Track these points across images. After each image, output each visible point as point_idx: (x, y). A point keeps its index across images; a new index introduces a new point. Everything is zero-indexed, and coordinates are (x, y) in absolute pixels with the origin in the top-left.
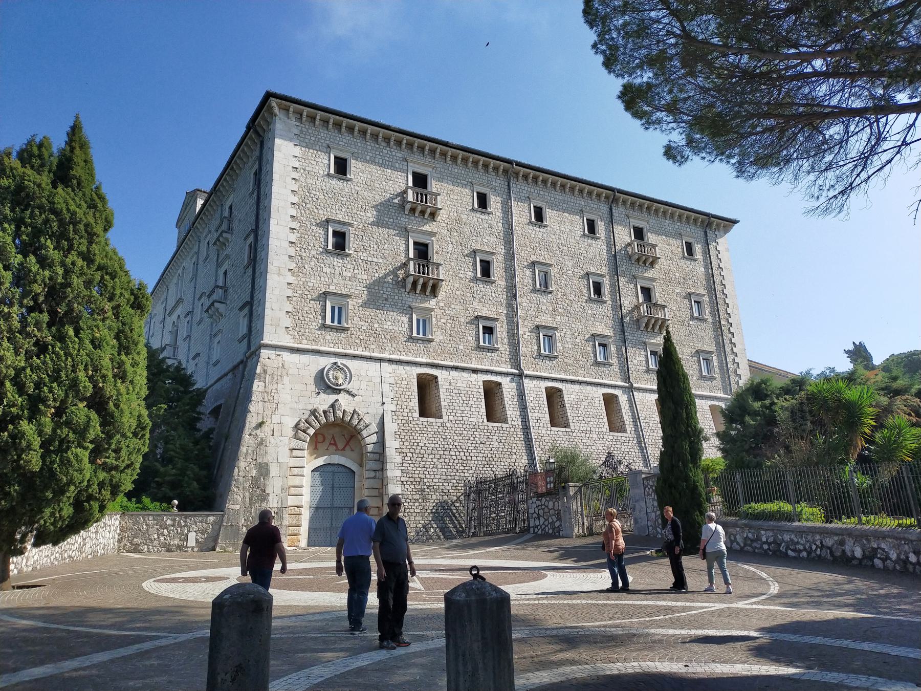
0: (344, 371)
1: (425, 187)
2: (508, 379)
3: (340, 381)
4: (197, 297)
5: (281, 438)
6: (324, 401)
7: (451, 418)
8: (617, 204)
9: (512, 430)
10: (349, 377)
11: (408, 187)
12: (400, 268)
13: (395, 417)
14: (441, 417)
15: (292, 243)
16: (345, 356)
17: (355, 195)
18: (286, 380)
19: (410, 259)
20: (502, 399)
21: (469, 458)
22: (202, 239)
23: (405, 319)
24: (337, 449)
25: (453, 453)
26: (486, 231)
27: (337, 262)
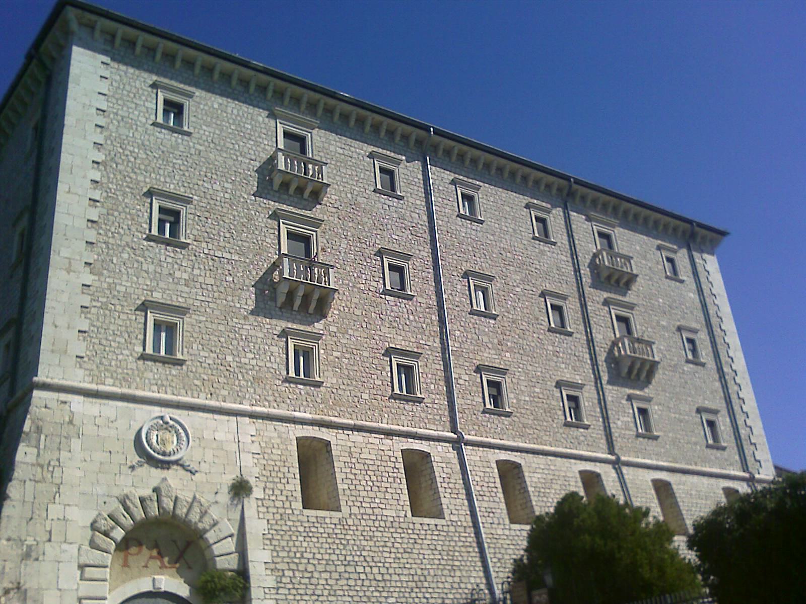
0: (177, 432)
3: (169, 448)
7: (355, 510)
9: (452, 529)
13: (262, 509)
14: (338, 509)
15: (93, 222)
18: (76, 444)
19: (281, 256)
20: (433, 480)
21: (387, 577)
25: (360, 569)
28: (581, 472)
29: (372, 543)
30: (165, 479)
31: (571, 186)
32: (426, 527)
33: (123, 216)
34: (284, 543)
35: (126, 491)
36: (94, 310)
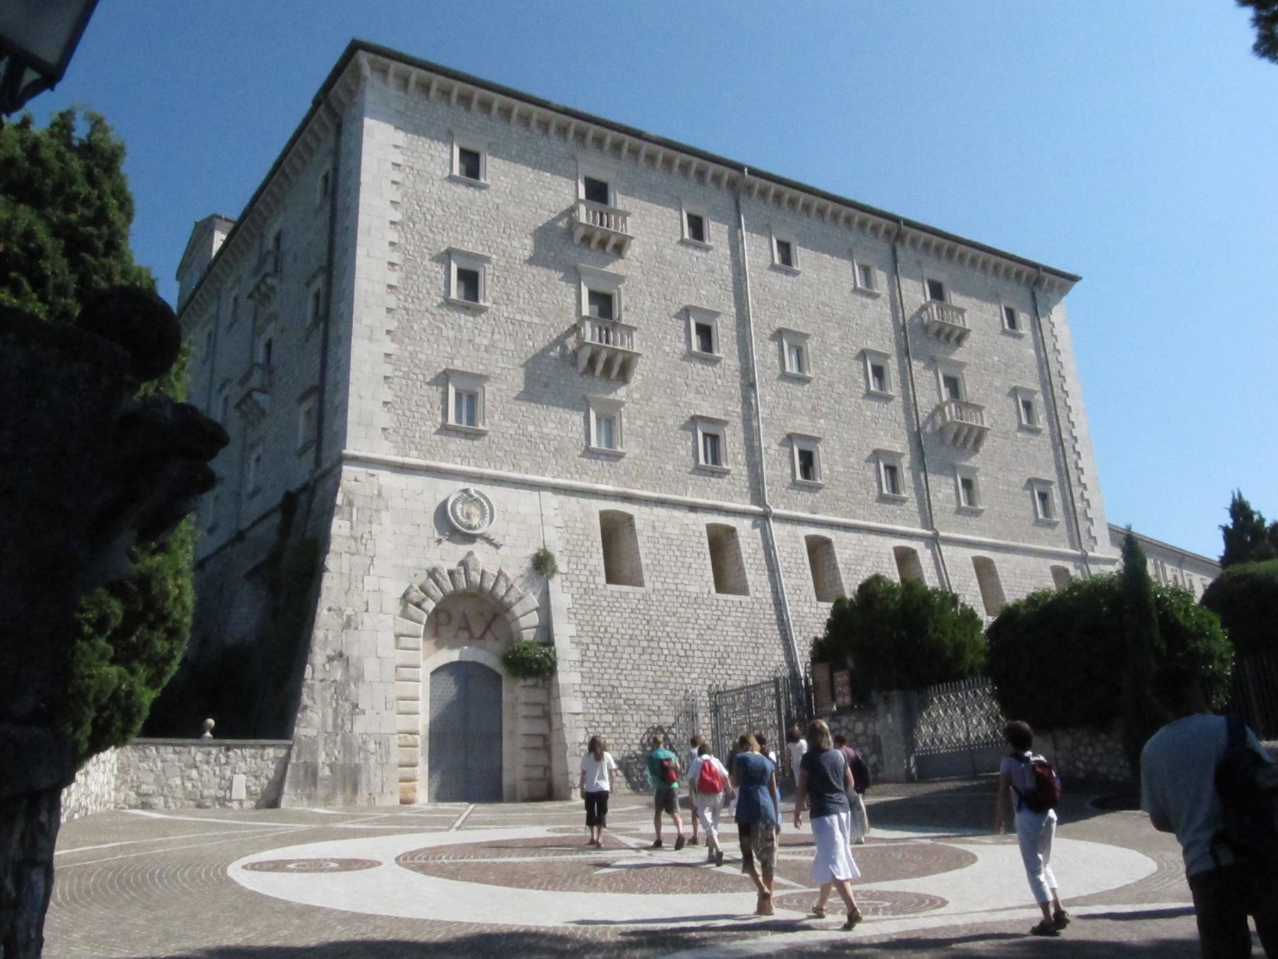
0: (481, 504)
2: (748, 522)
5: (381, 616)
6: (449, 556)
7: (658, 585)
8: (903, 242)
10: (488, 512)
11: (578, 201)
12: (568, 334)
14: (641, 584)
15: (390, 287)
16: (480, 478)
17: (493, 212)
18: (386, 517)
19: (583, 319)
21: (690, 653)
23: (578, 418)
24: (471, 637)
25: (663, 645)
26: (703, 278)
27: (465, 320)
29: (674, 619)
30: (470, 554)
31: (900, 229)
32: (730, 604)
33: (422, 279)
34: (587, 618)
35: (435, 564)
36: (396, 380)
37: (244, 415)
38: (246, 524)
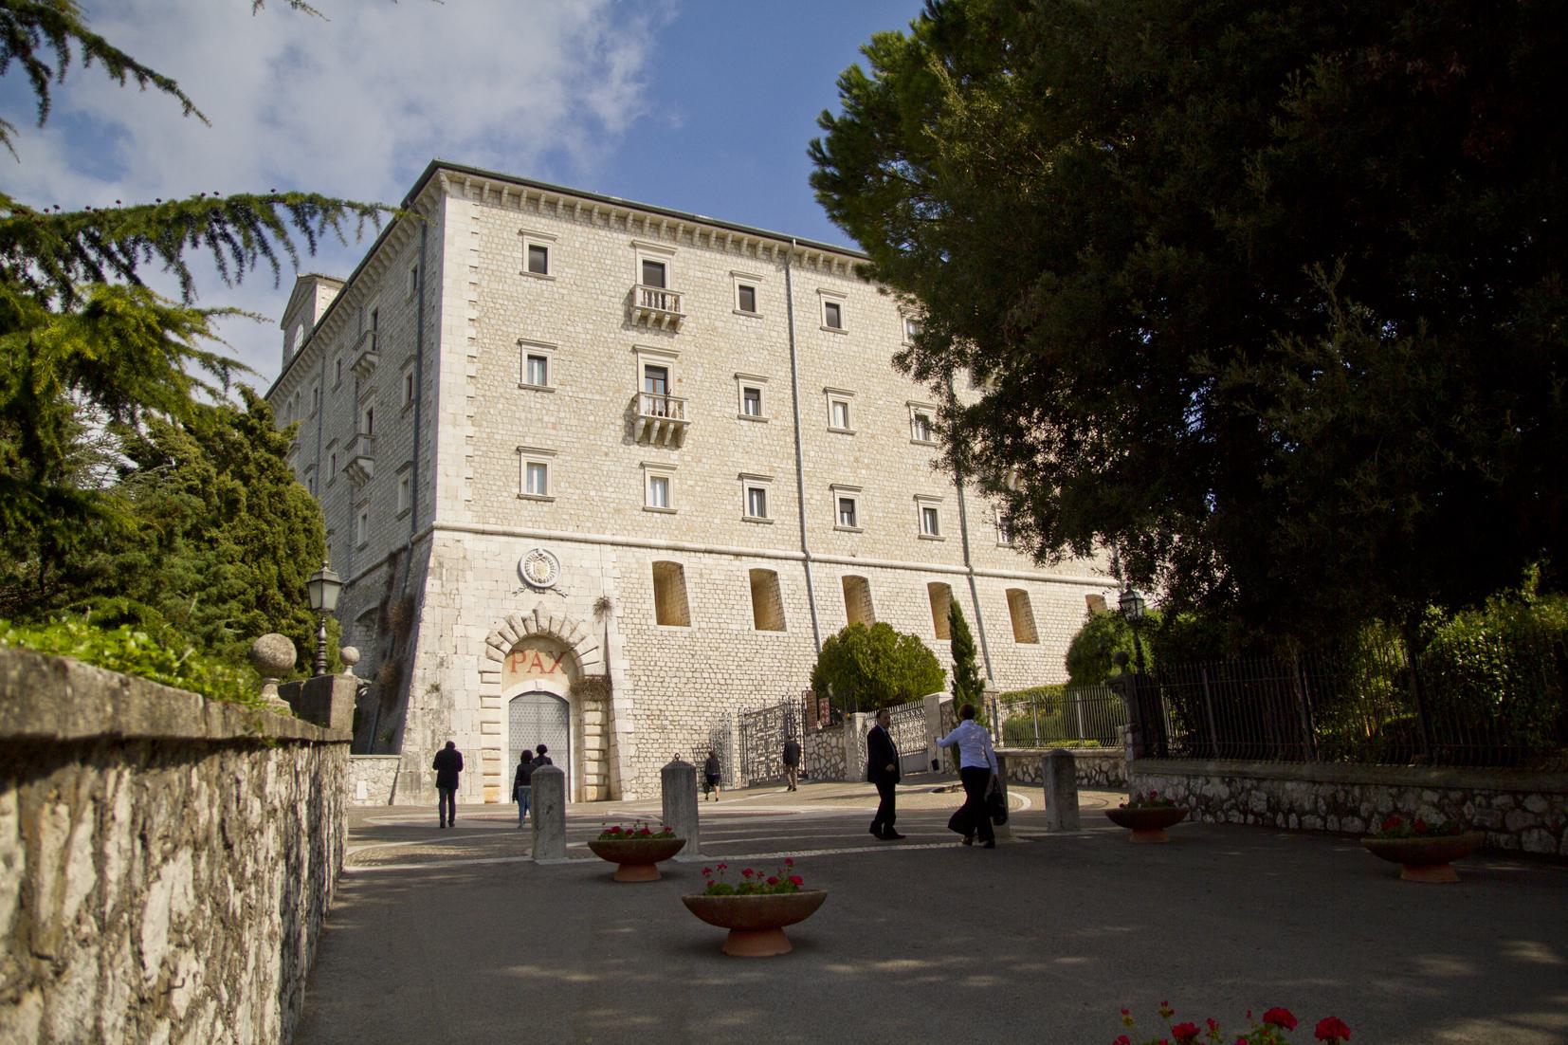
1: (663, 286)
4: (325, 443)
14: (688, 624)
18: (469, 575)
20: (778, 596)
22: (329, 353)
24: (543, 672)
28: (930, 585)
37: (352, 478)
38: (356, 574)
